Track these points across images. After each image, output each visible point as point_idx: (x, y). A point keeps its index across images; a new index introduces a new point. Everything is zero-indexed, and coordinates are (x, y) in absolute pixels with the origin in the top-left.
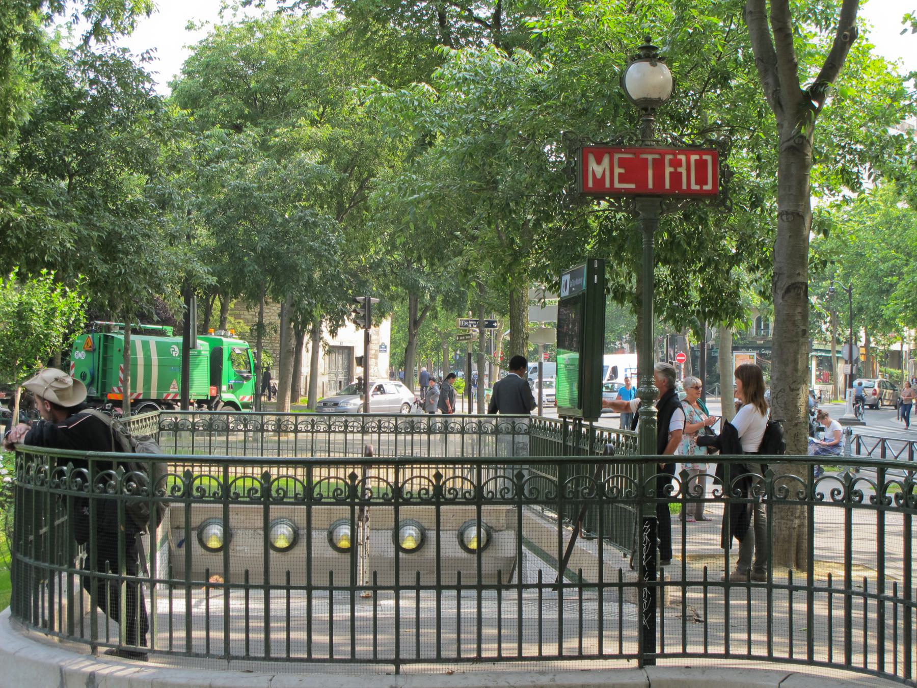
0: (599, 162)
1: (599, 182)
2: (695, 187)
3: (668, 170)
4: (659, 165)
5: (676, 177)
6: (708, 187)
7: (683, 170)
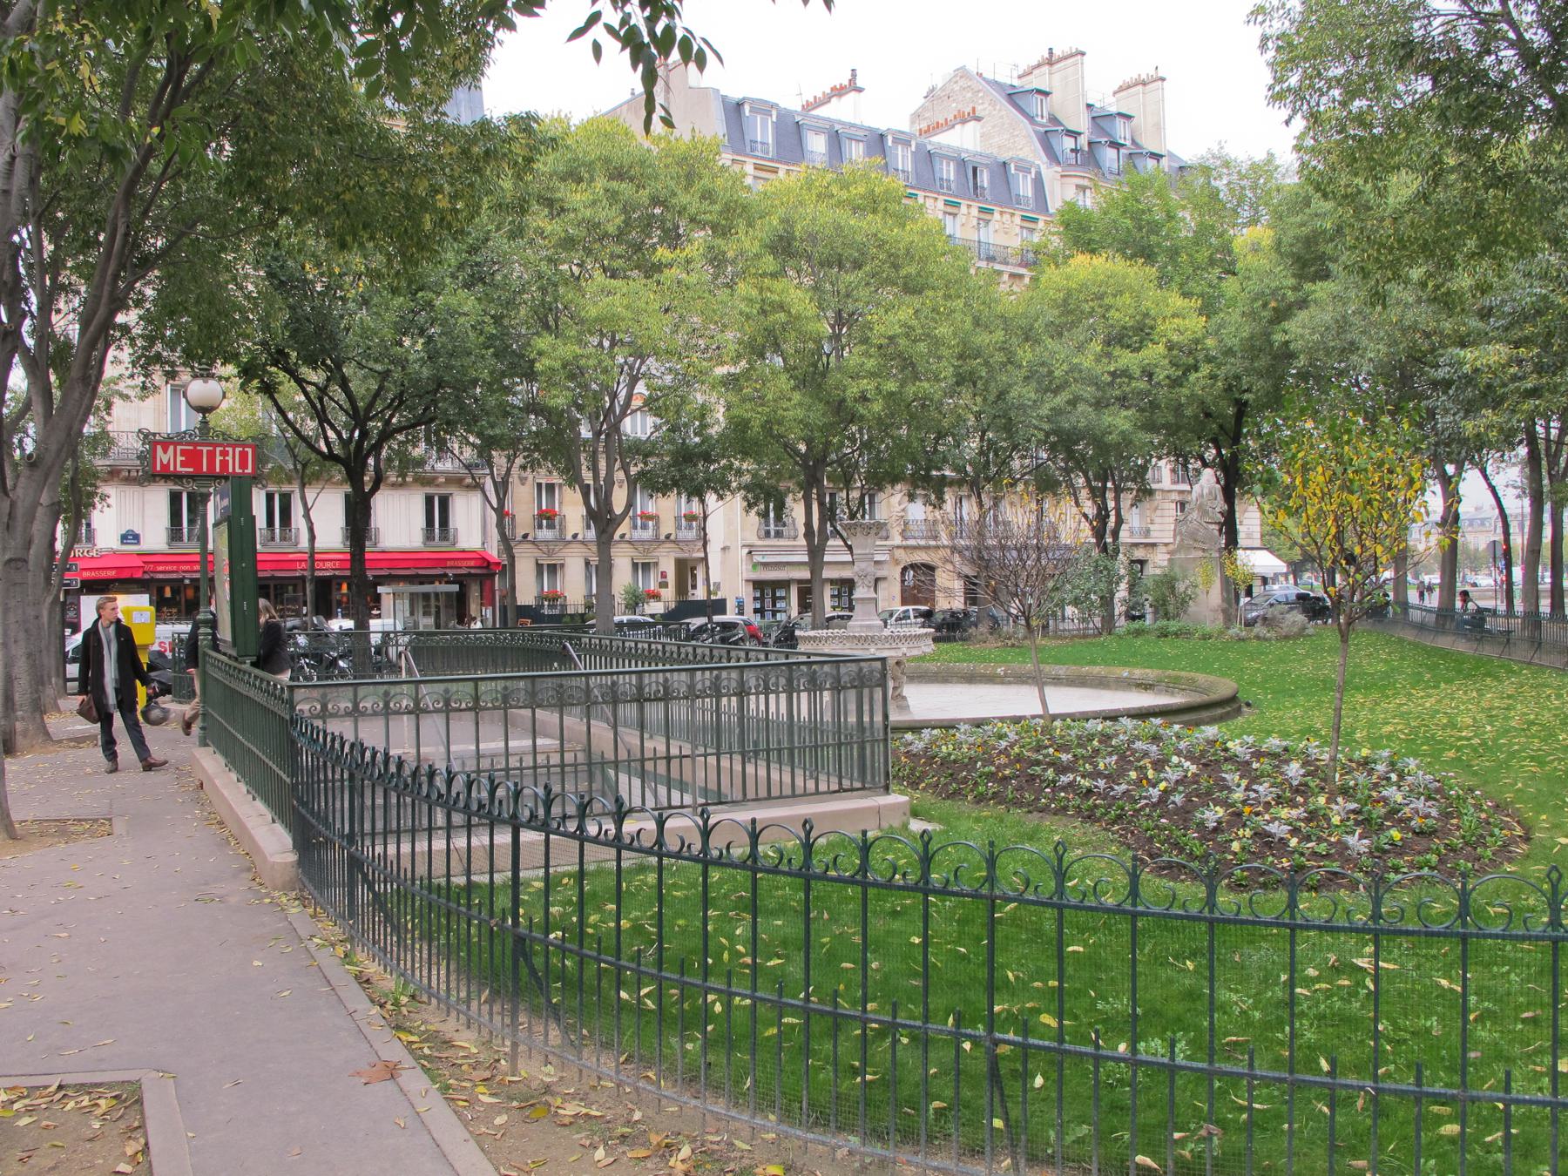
0: (165, 451)
1: (165, 467)
3: (219, 458)
4: (211, 455)
5: (224, 464)
7: (229, 458)
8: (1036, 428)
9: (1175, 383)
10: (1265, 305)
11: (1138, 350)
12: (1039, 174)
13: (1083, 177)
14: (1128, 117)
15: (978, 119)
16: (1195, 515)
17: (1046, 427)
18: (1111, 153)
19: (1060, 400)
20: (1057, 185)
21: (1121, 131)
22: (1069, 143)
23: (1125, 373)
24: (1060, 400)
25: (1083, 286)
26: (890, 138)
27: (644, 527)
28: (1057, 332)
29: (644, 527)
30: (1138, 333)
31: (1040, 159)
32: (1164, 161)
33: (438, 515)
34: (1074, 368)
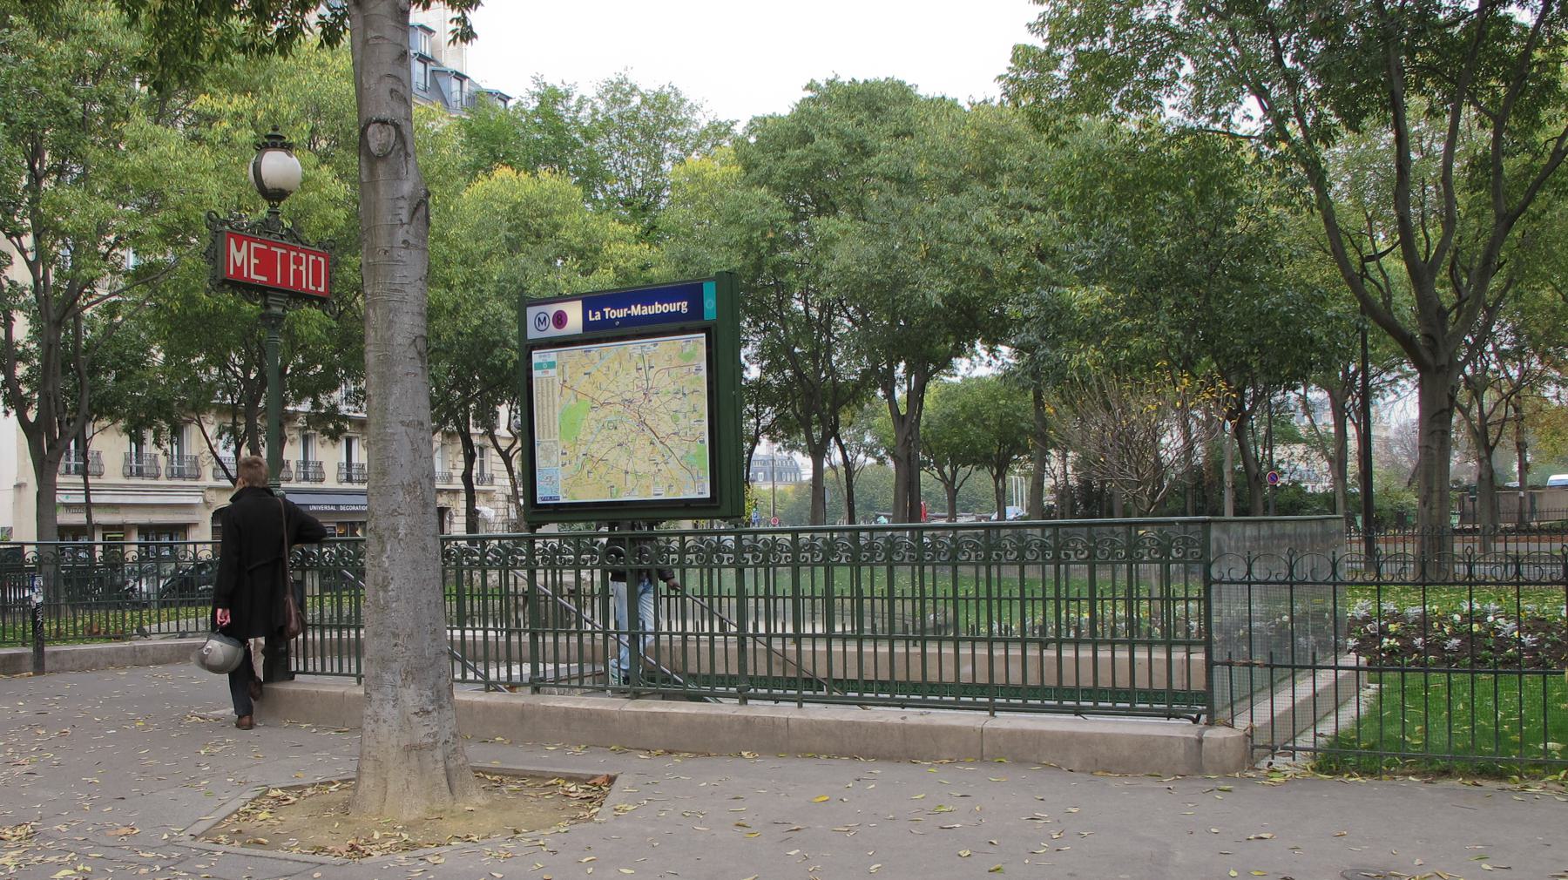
2: (312, 288)
3: (293, 267)
4: (285, 258)
6: (322, 289)
7: (303, 268)
10: (764, 234)
14: (430, 31)
32: (466, 83)
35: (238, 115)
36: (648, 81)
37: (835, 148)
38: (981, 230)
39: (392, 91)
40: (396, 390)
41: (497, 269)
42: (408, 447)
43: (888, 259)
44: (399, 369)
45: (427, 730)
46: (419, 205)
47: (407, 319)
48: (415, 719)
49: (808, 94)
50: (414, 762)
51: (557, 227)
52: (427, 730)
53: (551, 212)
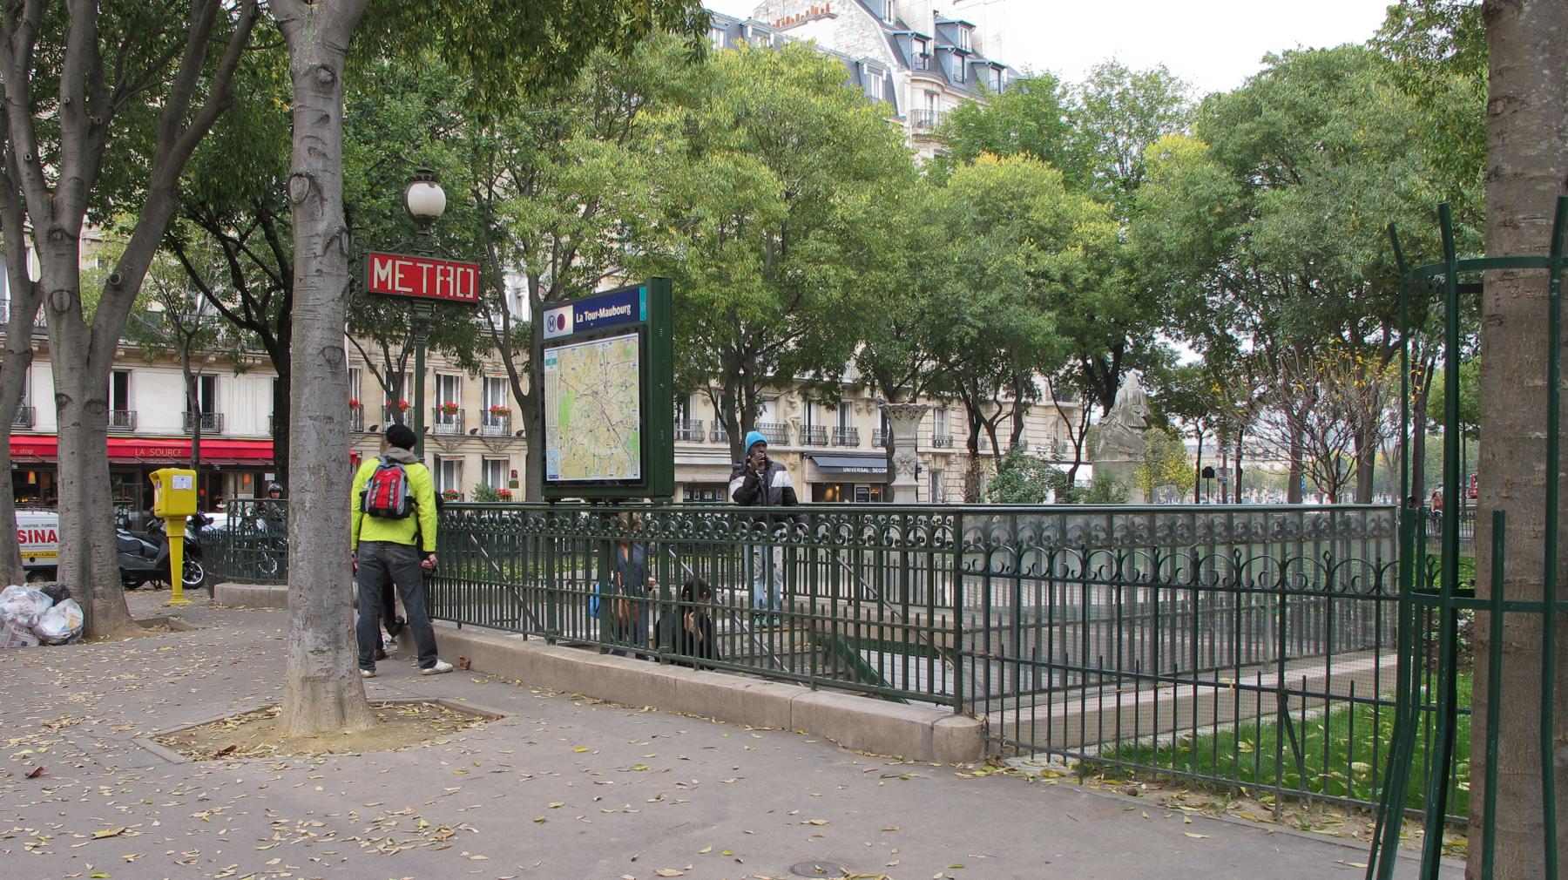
0: (383, 267)
1: (383, 284)
2: (459, 294)
3: (439, 279)
4: (432, 273)
5: (445, 285)
6: (471, 295)
7: (451, 279)
8: (970, 325)
9: (1088, 286)
10: (1210, 210)
11: (1058, 251)
12: (889, 76)
13: (932, 81)
14: (970, 26)
15: (833, 17)
16: (1119, 419)
17: (981, 324)
18: (956, 61)
19: (995, 297)
20: (908, 89)
21: (964, 40)
22: (917, 47)
23: (1045, 275)
24: (995, 297)
25: (1001, 186)
26: (750, 29)
27: (495, 423)
28: (986, 228)
29: (495, 423)
30: (1054, 235)
31: (892, 62)
32: (1004, 72)
33: (201, 411)
34: (1007, 266)
35: (669, 128)
36: (1139, 63)
37: (1284, 120)
38: (1407, 196)
39: (310, 149)
40: (307, 391)
41: (958, 251)
42: (315, 436)
43: (1319, 230)
44: (309, 374)
45: (320, 666)
46: (332, 240)
47: (317, 333)
48: (311, 656)
49: (1266, 66)
50: (308, 691)
51: (1027, 208)
52: (320, 666)
53: (1023, 194)
